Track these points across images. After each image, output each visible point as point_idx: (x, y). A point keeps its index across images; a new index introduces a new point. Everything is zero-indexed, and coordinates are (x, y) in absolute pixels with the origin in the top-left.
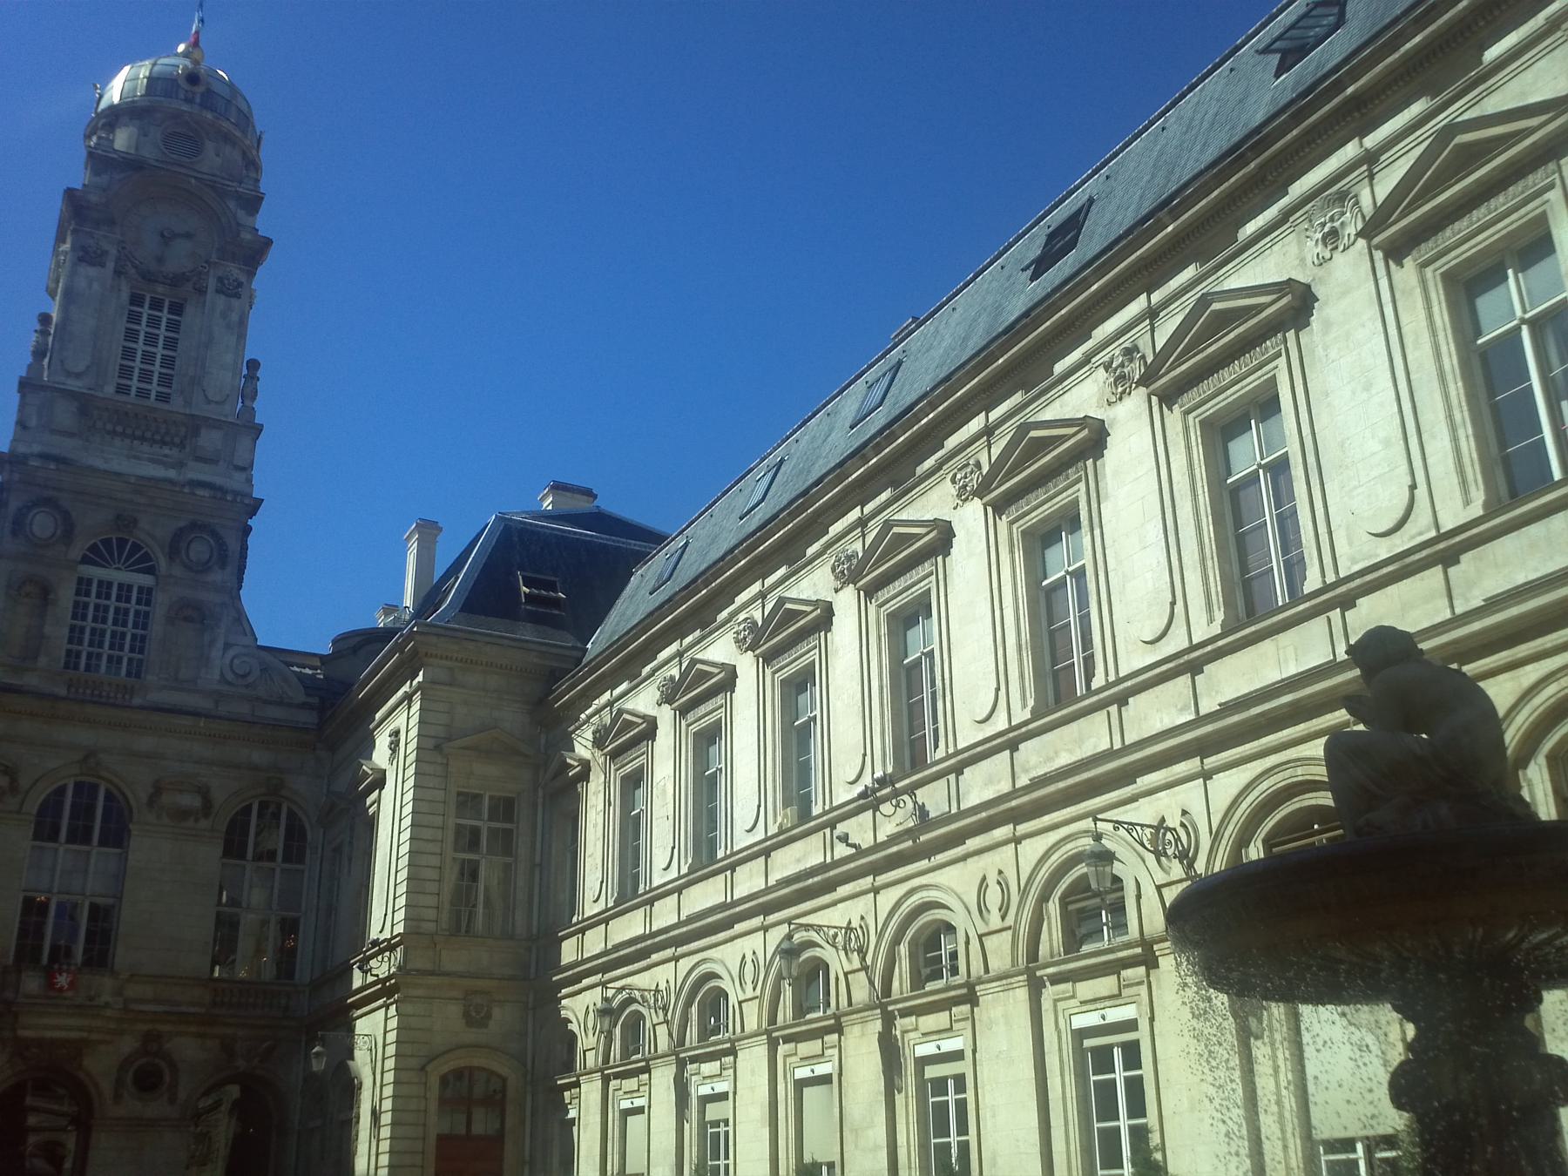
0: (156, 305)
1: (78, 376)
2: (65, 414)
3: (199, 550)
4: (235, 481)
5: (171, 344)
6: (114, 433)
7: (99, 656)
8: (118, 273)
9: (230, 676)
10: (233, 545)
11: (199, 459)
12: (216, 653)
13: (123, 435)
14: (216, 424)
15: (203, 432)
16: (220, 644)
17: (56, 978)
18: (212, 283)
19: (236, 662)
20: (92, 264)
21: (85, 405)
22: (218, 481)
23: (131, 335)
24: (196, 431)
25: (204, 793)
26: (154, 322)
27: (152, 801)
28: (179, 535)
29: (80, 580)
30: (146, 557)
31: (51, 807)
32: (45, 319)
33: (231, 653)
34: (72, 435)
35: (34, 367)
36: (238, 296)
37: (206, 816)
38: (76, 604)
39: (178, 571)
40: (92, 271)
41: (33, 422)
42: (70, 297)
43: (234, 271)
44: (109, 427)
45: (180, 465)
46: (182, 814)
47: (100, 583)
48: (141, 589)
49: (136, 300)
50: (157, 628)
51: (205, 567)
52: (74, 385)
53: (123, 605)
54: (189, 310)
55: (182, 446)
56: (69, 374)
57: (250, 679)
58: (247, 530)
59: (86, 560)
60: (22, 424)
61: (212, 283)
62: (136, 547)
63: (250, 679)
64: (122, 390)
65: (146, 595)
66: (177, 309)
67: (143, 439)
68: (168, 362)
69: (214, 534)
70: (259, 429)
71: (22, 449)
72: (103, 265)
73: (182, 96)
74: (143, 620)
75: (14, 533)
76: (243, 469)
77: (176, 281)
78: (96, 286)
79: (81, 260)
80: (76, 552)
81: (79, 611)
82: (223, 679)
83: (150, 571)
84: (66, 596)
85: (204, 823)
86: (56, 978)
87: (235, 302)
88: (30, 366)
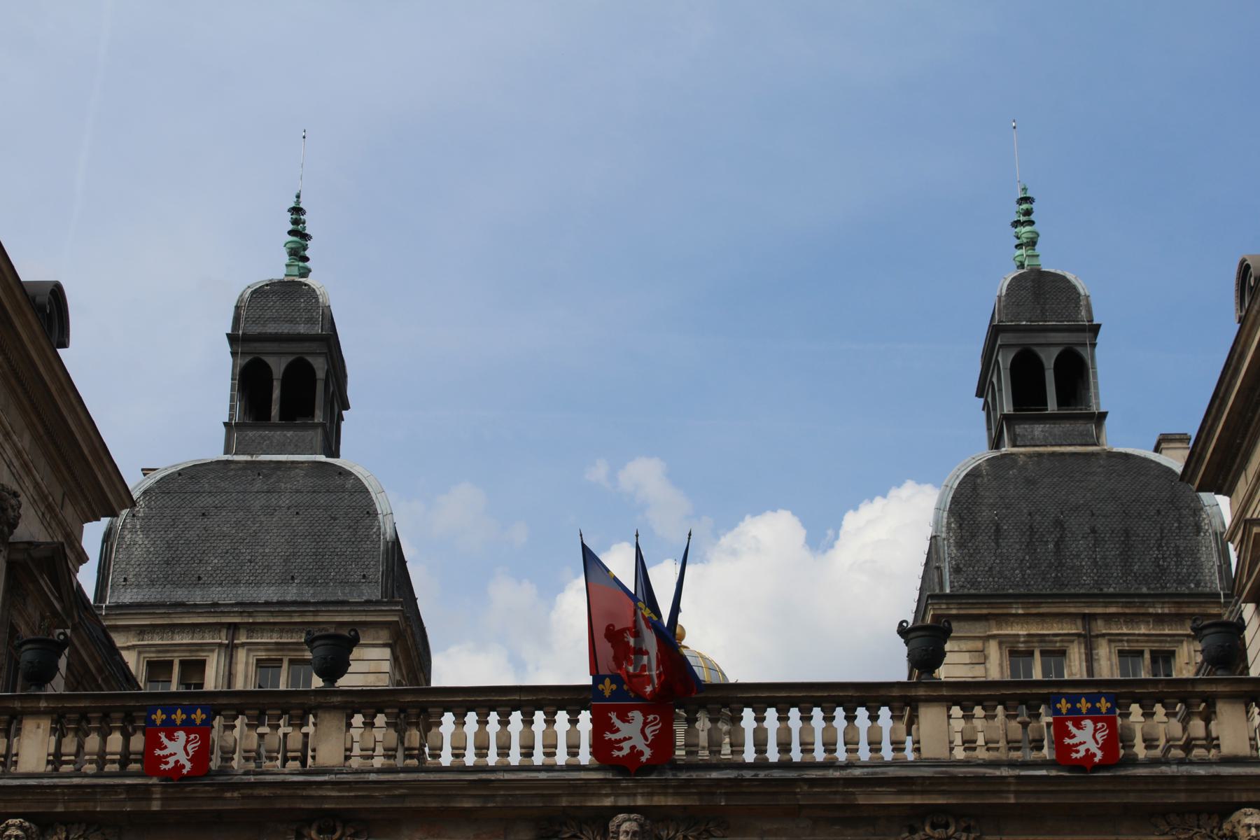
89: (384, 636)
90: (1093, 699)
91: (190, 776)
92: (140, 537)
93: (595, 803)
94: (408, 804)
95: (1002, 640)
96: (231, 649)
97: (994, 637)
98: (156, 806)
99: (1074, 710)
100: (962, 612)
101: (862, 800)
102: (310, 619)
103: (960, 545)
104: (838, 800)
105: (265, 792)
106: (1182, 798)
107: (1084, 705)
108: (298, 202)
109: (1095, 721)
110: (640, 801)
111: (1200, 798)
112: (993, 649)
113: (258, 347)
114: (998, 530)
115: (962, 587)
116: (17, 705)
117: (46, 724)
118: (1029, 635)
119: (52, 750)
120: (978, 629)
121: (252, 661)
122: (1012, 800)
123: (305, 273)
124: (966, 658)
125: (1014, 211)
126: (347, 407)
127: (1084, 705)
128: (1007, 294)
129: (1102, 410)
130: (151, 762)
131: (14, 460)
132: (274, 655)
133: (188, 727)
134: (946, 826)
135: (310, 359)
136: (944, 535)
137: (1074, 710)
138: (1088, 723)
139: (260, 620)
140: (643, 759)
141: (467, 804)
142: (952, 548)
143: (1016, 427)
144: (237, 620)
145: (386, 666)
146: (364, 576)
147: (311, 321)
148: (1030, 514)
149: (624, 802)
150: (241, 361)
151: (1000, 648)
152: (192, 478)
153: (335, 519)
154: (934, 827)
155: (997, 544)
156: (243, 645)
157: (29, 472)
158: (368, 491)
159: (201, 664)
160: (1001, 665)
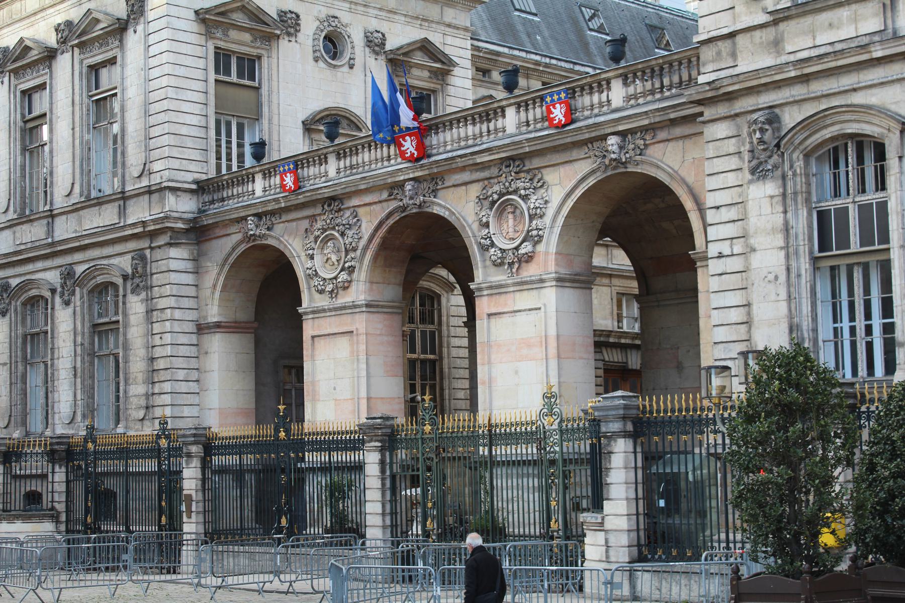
90: (559, 93)
91: (294, 191)
93: (397, 179)
94: (347, 190)
98: (283, 205)
99: (552, 100)
101: (479, 161)
104: (471, 162)
105: (309, 194)
106: (587, 136)
107: (556, 97)
109: (560, 104)
110: (411, 176)
111: (593, 135)
122: (527, 150)
127: (556, 97)
130: (283, 186)
131: (381, 13)
133: (290, 171)
134: (509, 166)
137: (552, 100)
140: (415, 156)
141: (363, 187)
149: (407, 177)
154: (507, 167)
157: (395, 13)
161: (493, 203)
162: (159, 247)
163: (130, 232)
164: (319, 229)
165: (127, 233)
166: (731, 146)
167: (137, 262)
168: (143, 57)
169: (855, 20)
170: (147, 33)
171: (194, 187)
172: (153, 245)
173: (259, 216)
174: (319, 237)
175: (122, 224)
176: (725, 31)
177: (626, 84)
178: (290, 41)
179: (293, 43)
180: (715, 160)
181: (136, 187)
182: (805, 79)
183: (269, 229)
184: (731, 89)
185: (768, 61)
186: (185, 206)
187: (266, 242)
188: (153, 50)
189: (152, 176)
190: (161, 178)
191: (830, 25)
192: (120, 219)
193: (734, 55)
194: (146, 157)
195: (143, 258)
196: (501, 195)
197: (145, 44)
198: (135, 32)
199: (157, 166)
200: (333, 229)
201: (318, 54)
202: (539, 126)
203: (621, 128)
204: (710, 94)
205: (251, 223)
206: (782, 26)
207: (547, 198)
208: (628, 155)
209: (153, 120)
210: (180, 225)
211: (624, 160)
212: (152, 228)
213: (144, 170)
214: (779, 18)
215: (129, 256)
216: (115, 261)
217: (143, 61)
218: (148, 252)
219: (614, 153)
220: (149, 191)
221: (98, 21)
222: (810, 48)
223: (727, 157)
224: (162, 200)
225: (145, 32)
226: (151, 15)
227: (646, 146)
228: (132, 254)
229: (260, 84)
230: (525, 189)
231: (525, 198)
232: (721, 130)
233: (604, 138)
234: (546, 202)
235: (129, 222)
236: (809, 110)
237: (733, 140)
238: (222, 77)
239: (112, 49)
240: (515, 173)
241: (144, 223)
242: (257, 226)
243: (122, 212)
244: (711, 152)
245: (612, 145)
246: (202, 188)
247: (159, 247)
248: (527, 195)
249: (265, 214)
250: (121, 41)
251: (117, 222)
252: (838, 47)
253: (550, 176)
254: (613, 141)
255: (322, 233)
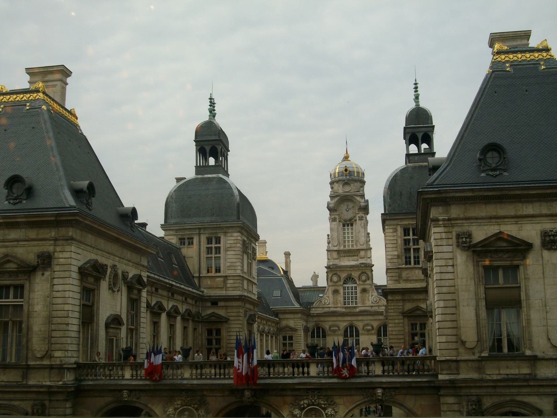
0: (348, 225)
1: (336, 246)
2: (335, 255)
3: (364, 278)
4: (368, 261)
5: (352, 233)
6: (344, 256)
7: (349, 301)
8: (339, 221)
9: (373, 302)
10: (370, 275)
11: (361, 258)
12: (370, 298)
13: (346, 256)
14: (363, 250)
15: (361, 252)
16: (371, 296)
17: (342, 372)
18: (358, 218)
19: (374, 299)
20: (334, 221)
21: (338, 252)
22: (365, 262)
23: (344, 233)
24: (359, 253)
25: (372, 327)
26: (348, 229)
27: (363, 329)
28: (360, 275)
29: (344, 287)
30: (355, 280)
31: (346, 331)
32: (328, 235)
33: (373, 297)
34: (337, 259)
35: (328, 247)
36: (363, 220)
37: (373, 330)
38: (344, 292)
39: (361, 283)
40: (335, 223)
41: (330, 258)
42: (331, 229)
43: (361, 214)
44: (343, 255)
45: (358, 260)
46: (368, 330)
47: (347, 287)
48: (355, 287)
49: (344, 225)
50: (359, 295)
51: (365, 281)
52: (336, 248)
53: (352, 291)
54: (354, 225)
55: (357, 256)
56: (334, 246)
57: (377, 302)
58: (372, 271)
59: (344, 283)
60: (328, 259)
61: (358, 218)
62: (353, 279)
63: (377, 302)
64: (345, 246)
65: (356, 288)
66: (352, 225)
67: (350, 256)
68: (352, 237)
69: (366, 273)
70: (371, 249)
71: (329, 264)
72: (336, 221)
73: (345, 175)
74: (356, 293)
75: (331, 281)
76: (370, 258)
77: (350, 220)
78: (336, 226)
79: (332, 221)
80: (342, 283)
81: (344, 293)
82: (372, 303)
83: (356, 283)
84: (342, 291)
85: (373, 332)
86: (342, 372)
87: (362, 221)
88: (327, 246)
89: (238, 229)
92: (174, 205)
95: (401, 225)
96: (199, 234)
97: (399, 224)
100: (391, 218)
102: (219, 226)
103: (391, 198)
108: (211, 96)
112: (399, 228)
113: (202, 143)
114: (401, 193)
115: (391, 211)
116: (123, 364)
117: (129, 368)
118: (409, 224)
119: (131, 374)
120: (395, 222)
121: (205, 237)
123: (214, 116)
124: (391, 230)
125: (414, 86)
126: (229, 151)
128: (408, 117)
129: (435, 151)
132: (210, 236)
134: (314, 392)
135: (216, 146)
136: (386, 196)
138: (346, 369)
139: (206, 226)
142: (388, 199)
143: (410, 157)
144: (200, 227)
145: (239, 238)
146: (232, 214)
147: (215, 135)
148: (410, 188)
150: (198, 148)
151: (401, 227)
152: (186, 186)
153: (224, 197)
154: (312, 392)
155: (401, 198)
156: (202, 233)
158: (232, 188)
159: (192, 238)
160: (401, 233)
161: (304, 408)
162: (57, 401)
163: (36, 390)
164: (179, 404)
165: (32, 390)
166: (456, 407)
167: (39, 407)
168: (49, 290)
169: (519, 368)
170: (52, 277)
171: (75, 366)
172: (52, 399)
173: (131, 391)
174: (178, 408)
175: (24, 383)
176: (454, 358)
177: (383, 365)
178: (103, 280)
179: (104, 281)
180: (447, 412)
181: (38, 363)
182: (494, 387)
183: (137, 399)
184: (461, 385)
185: (474, 375)
186: (69, 378)
187: (134, 405)
188: (56, 288)
189: (53, 359)
190: (61, 361)
191: (507, 367)
192: (23, 379)
193: (458, 369)
194: (48, 347)
195: (43, 406)
196: (308, 405)
197: (51, 282)
198: (43, 274)
199: (58, 354)
200: (190, 406)
201: (111, 286)
202: (331, 375)
203: (384, 386)
204: (449, 385)
205: (125, 393)
206: (483, 363)
207: (337, 410)
208: (386, 398)
209: (53, 327)
210: (73, 389)
211: (384, 400)
212: (56, 390)
213: (46, 354)
214: (482, 359)
215: (31, 403)
216: (16, 403)
217: (49, 293)
218: (47, 403)
219: (380, 396)
220: (51, 367)
221: (9, 261)
222: (497, 374)
223: (453, 412)
224: (62, 376)
225: (51, 276)
226: (57, 268)
227: (395, 395)
228: (36, 402)
229: (93, 304)
230: (324, 404)
231: (325, 409)
232: (451, 400)
233: (375, 388)
234: (336, 412)
235: (31, 382)
236: (496, 400)
237: (457, 405)
238: (85, 303)
239: (20, 280)
240: (318, 396)
241: (50, 387)
242: (129, 396)
243: (25, 376)
244: (445, 408)
245: (380, 393)
246: (79, 367)
247: (57, 401)
248: (324, 408)
249: (135, 390)
250: (29, 277)
251: (21, 381)
252: (510, 376)
253: (338, 400)
254: (379, 391)
255: (181, 407)
